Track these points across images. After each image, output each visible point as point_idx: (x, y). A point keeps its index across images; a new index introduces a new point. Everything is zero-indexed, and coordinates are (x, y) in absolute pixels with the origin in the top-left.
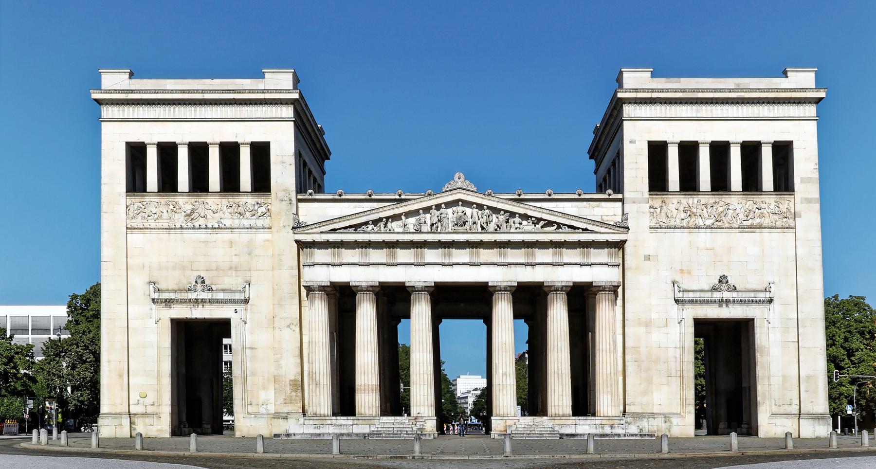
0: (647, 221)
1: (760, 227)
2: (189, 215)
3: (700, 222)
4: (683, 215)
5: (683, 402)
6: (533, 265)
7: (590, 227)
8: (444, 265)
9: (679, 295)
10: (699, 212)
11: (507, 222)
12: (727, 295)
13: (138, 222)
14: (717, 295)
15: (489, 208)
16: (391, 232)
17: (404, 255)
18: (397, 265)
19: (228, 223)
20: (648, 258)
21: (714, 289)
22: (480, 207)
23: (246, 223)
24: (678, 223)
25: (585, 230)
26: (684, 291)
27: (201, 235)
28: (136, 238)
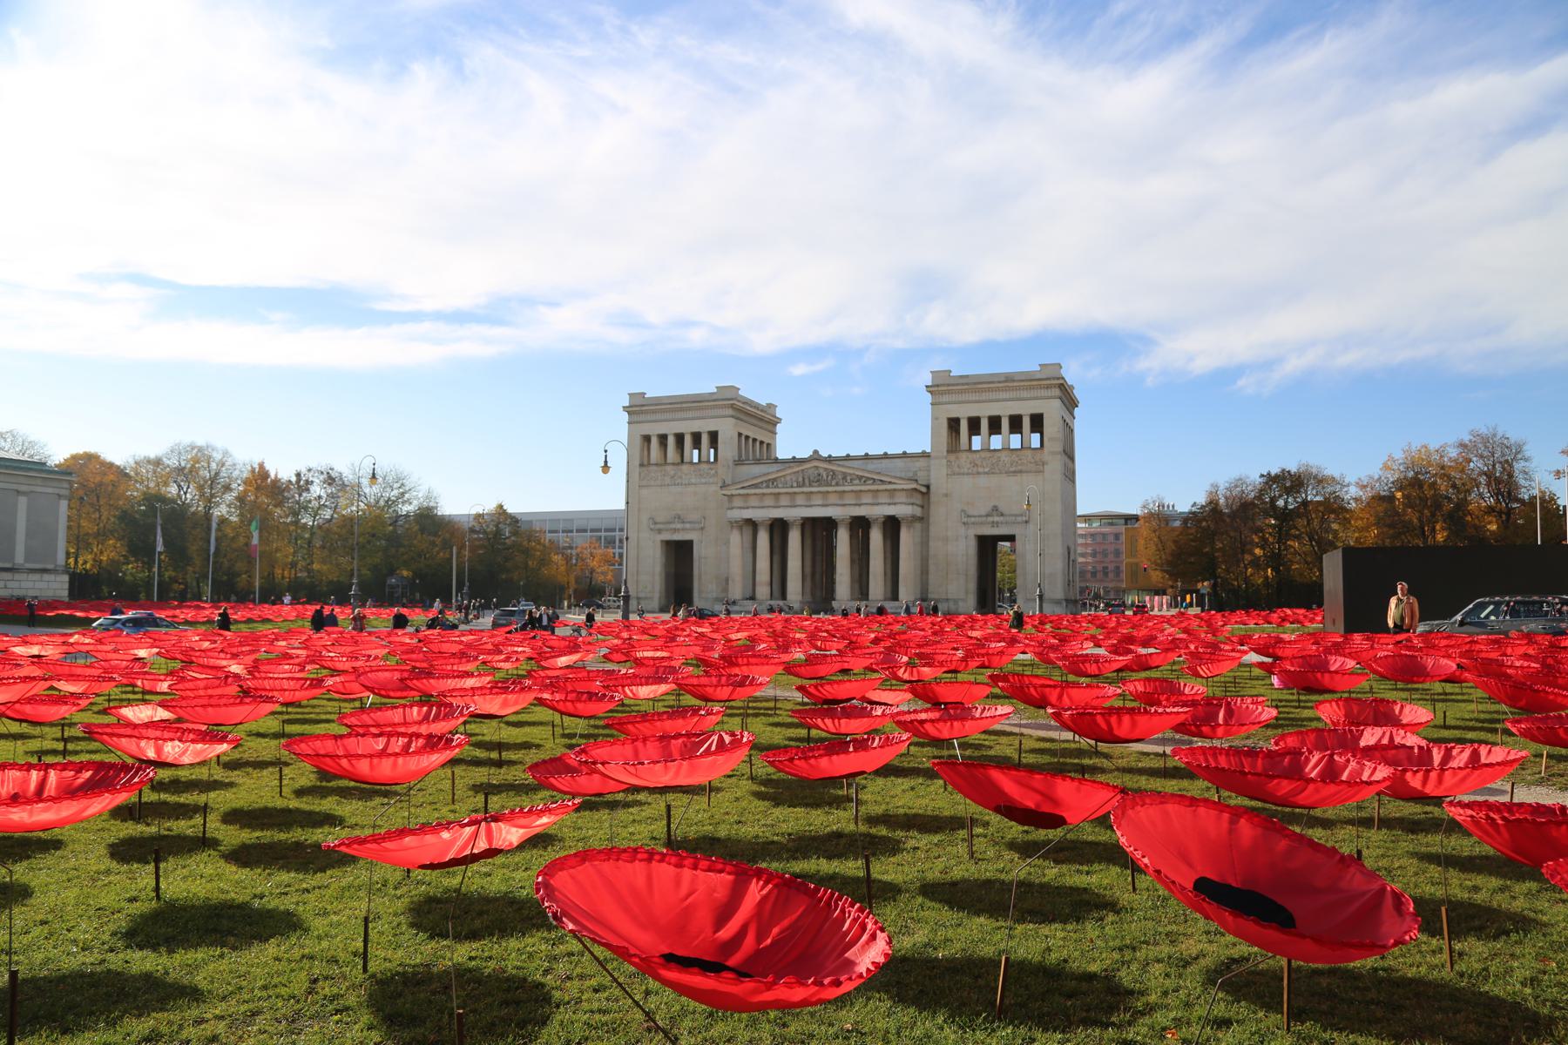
0: (944, 471)
1: (1021, 472)
2: (672, 477)
3: (981, 470)
4: (969, 466)
5: (967, 593)
6: (860, 505)
7: (893, 481)
8: (806, 506)
9: (965, 520)
10: (979, 463)
11: (844, 478)
12: (996, 519)
13: (644, 483)
14: (990, 519)
15: (832, 471)
16: (777, 487)
17: (784, 501)
18: (779, 507)
19: (693, 481)
20: (946, 495)
21: (987, 515)
22: (826, 469)
23: (703, 480)
24: (966, 470)
25: (890, 483)
26: (968, 516)
27: (679, 489)
28: (644, 492)
